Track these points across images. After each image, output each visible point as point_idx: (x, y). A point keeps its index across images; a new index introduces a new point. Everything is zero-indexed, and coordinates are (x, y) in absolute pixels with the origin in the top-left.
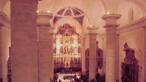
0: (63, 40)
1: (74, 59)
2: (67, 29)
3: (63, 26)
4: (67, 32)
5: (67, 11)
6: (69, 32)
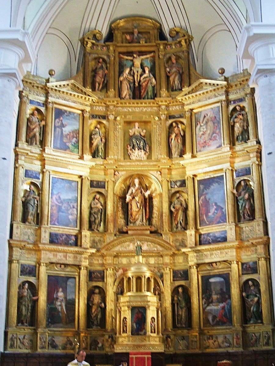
0: (111, 134)
1: (205, 280)
2: (141, 53)
3: (105, 33)
4: (137, 70)
6: (152, 70)
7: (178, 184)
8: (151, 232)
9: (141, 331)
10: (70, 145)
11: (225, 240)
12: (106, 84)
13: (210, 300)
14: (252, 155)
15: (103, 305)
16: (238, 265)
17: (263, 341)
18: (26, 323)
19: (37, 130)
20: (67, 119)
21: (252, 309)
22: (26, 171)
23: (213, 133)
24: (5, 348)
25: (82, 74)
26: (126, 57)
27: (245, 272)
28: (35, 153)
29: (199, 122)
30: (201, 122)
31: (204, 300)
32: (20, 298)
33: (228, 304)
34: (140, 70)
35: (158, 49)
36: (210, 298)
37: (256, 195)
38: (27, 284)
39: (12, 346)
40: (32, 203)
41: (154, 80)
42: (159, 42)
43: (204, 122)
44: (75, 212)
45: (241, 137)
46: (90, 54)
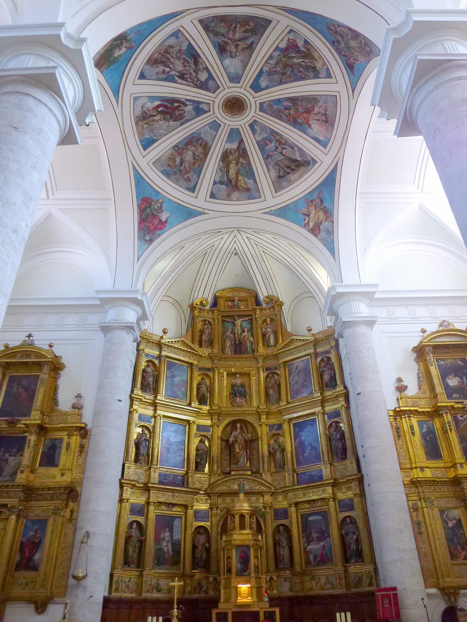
1: (305, 517)
3: (210, 300)
5: (225, 157)
7: (276, 427)
8: (253, 473)
9: (245, 571)
10: (179, 394)
11: (321, 478)
12: (212, 342)
13: (311, 539)
14: (340, 399)
15: (207, 545)
16: (335, 502)
17: (365, 581)
18: (133, 563)
19: (151, 379)
20: (178, 371)
21: (352, 547)
22: (140, 415)
23: (305, 382)
24: (110, 592)
25: (191, 334)
26: (228, 320)
27: (342, 510)
28: (149, 399)
29: (292, 373)
30: (294, 371)
31: (305, 539)
32: (128, 538)
33: (327, 542)
34: (240, 331)
35: (255, 313)
36: (310, 538)
37: (347, 435)
38: (135, 524)
39: (117, 590)
40: (144, 445)
41: (252, 339)
42: (256, 307)
43: (296, 373)
44: (183, 454)
45: (329, 384)
46: (198, 317)
